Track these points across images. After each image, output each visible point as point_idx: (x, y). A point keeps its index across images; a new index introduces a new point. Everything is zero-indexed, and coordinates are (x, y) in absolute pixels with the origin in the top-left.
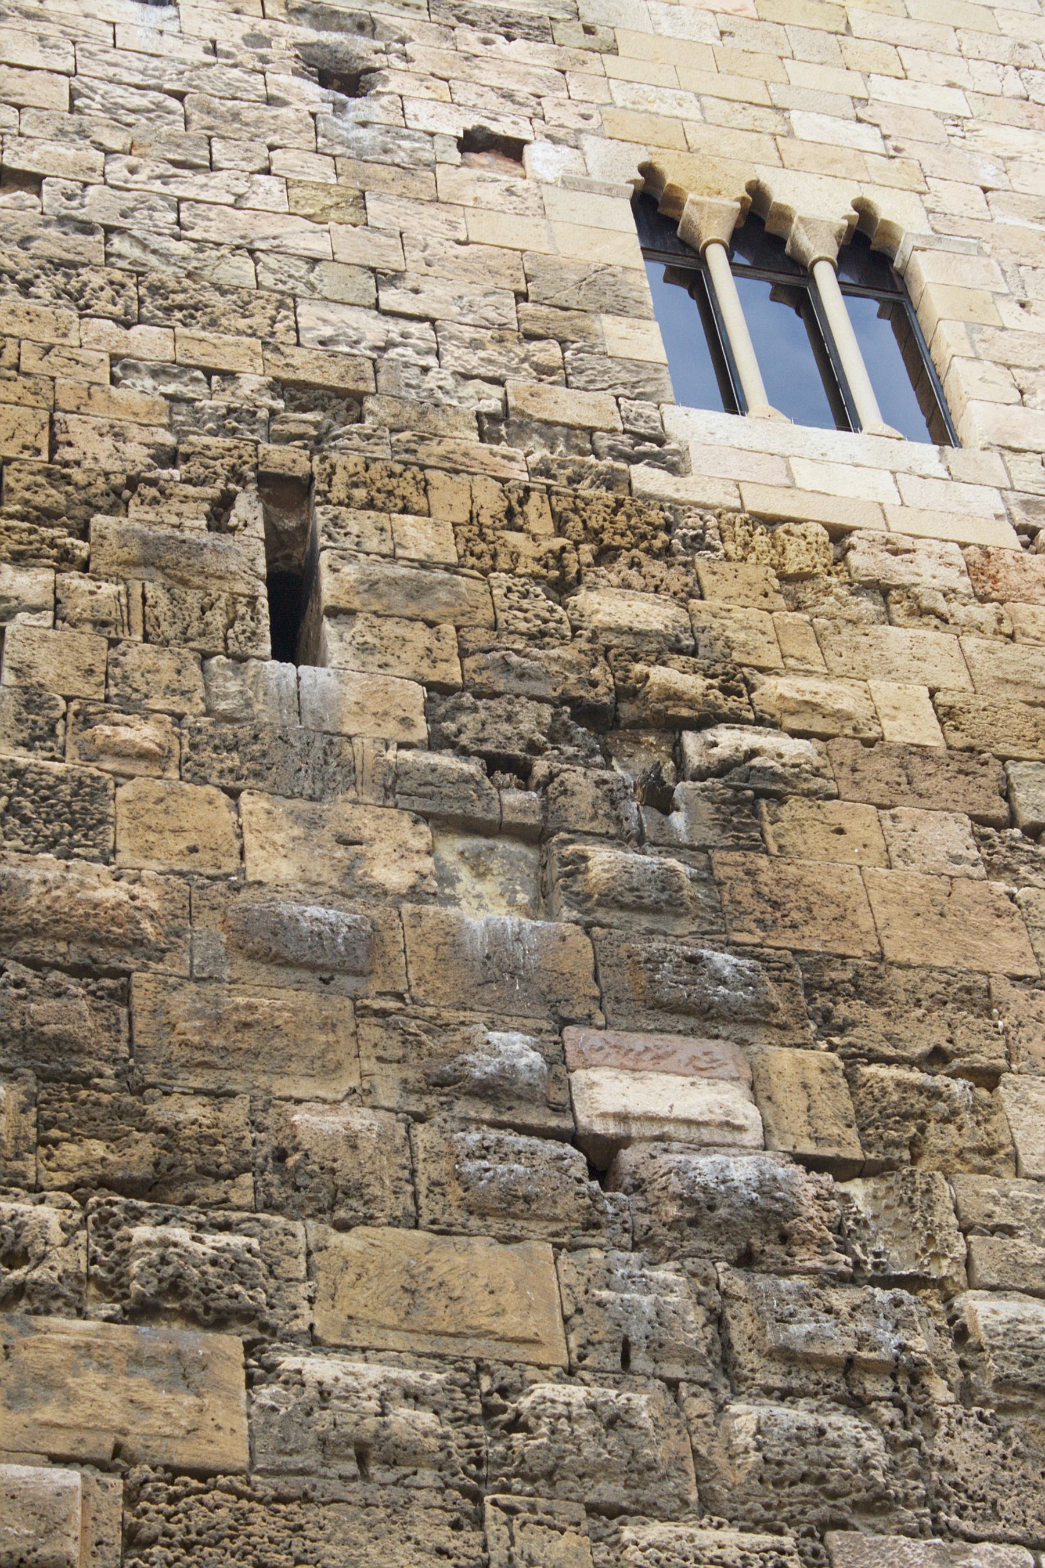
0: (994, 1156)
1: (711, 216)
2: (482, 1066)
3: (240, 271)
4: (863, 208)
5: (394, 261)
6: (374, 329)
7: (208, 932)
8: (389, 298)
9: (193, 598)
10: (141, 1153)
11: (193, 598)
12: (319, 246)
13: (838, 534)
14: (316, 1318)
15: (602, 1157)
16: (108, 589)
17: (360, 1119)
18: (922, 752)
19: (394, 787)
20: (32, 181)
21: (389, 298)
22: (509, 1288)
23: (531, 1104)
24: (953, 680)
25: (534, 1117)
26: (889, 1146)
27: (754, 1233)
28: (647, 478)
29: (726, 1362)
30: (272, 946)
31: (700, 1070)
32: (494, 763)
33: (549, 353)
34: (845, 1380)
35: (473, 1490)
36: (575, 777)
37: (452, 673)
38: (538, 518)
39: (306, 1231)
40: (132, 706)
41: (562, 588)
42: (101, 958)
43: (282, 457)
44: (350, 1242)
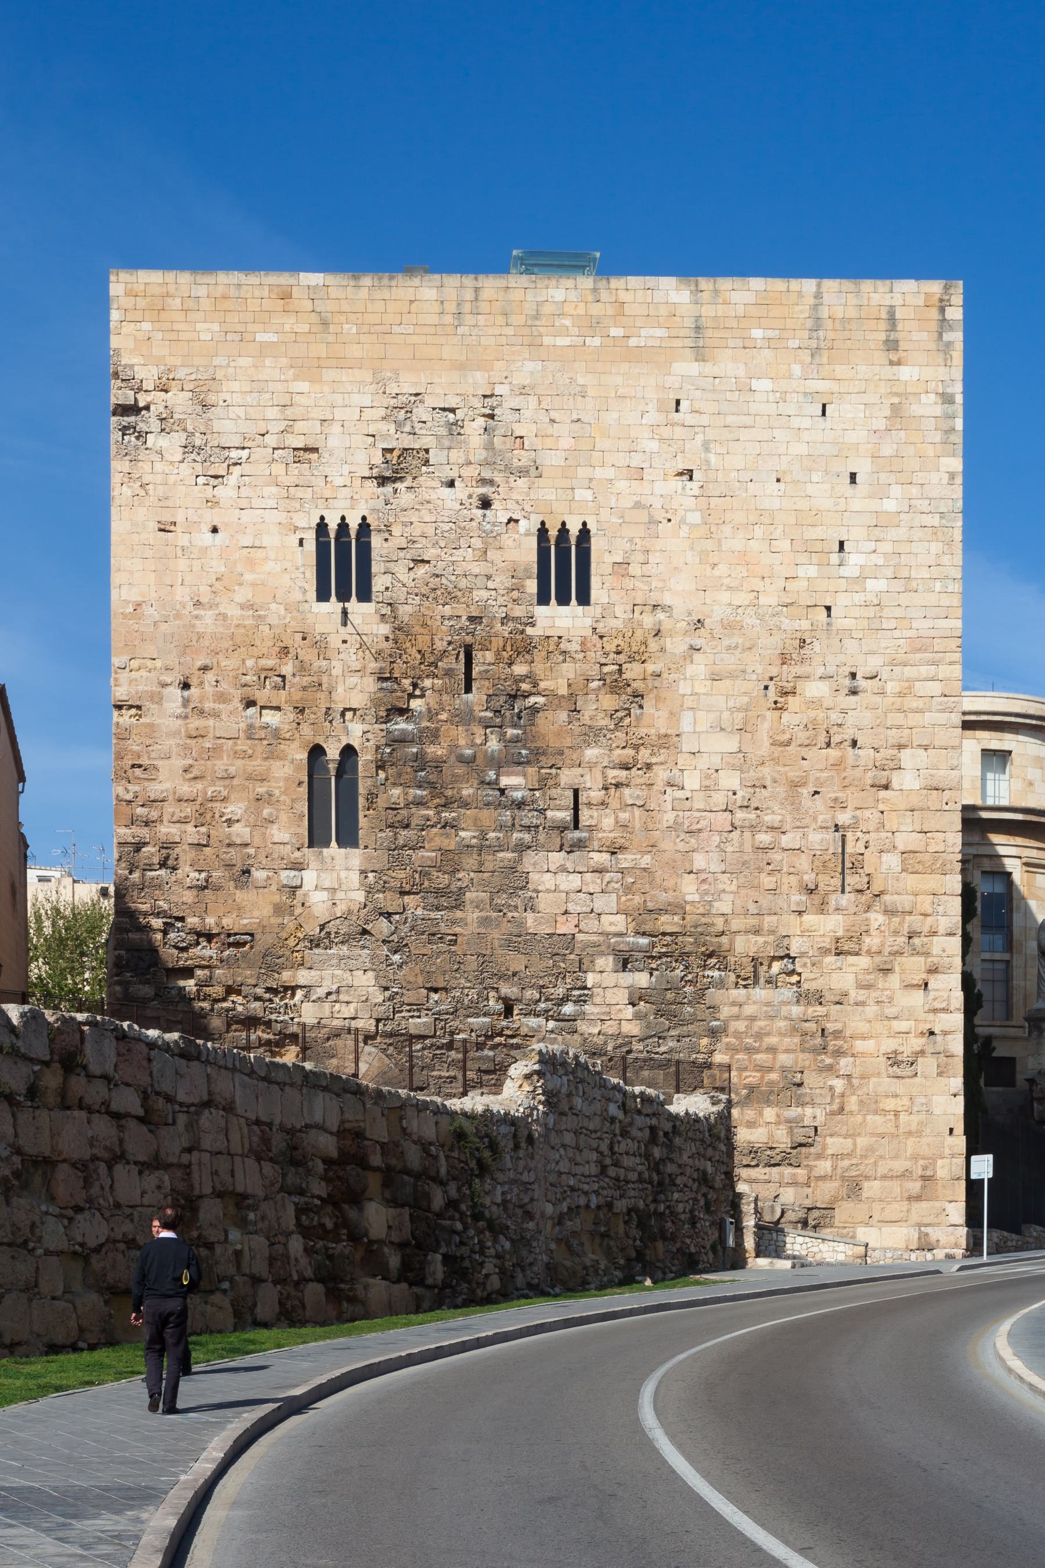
0: (557, 785)
1: (553, 533)
2: (488, 779)
3: (463, 583)
4: (584, 524)
5: (491, 572)
6: (485, 594)
7: (453, 758)
8: (490, 584)
9: (453, 680)
10: (442, 801)
11: (453, 680)
12: (476, 570)
13: (560, 637)
14: (463, 826)
15: (502, 791)
16: (441, 682)
17: (471, 791)
18: (563, 696)
19: (481, 720)
20: (428, 562)
21: (490, 584)
22: (487, 816)
23: (493, 784)
24: (572, 676)
25: (494, 786)
26: (543, 784)
27: (520, 805)
28: (529, 630)
29: (513, 825)
30: (462, 760)
31: (517, 774)
32: (496, 711)
33: (515, 594)
34: (528, 828)
35: (480, 849)
36: (508, 714)
37: (491, 692)
38: (509, 648)
39: (463, 811)
40: (443, 710)
41: (510, 665)
42: (438, 765)
43: (469, 639)
44: (468, 812)
